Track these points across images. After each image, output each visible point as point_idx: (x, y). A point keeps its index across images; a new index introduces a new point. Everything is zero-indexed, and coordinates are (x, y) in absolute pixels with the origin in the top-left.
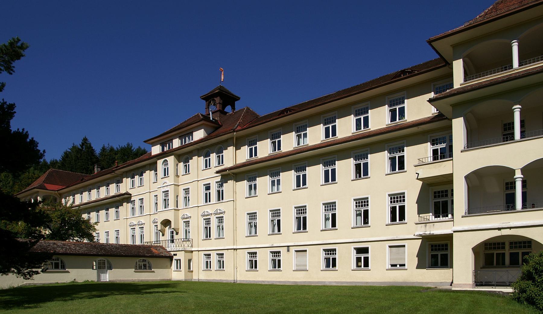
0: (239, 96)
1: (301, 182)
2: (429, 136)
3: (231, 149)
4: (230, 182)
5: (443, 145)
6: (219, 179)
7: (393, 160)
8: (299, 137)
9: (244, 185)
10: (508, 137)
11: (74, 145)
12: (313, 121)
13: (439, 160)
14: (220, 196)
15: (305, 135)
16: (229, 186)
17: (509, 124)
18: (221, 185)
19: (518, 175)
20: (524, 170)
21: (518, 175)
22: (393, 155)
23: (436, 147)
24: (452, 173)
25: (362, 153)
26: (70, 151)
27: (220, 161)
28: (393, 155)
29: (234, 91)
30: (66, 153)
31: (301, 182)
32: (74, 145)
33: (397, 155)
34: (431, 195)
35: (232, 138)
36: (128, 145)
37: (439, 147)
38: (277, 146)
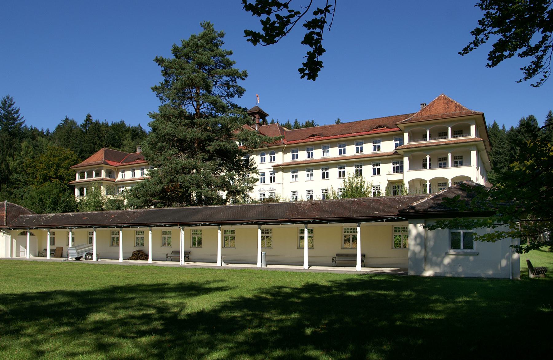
0: (268, 114)
1: (325, 176)
2: (392, 160)
3: (281, 154)
4: (280, 173)
5: (398, 165)
6: (272, 170)
7: (374, 169)
8: (324, 152)
9: (290, 174)
10: (424, 166)
11: (67, 117)
12: (333, 144)
13: (396, 173)
14: (273, 180)
15: (328, 151)
16: (279, 175)
17: (425, 159)
18: (273, 174)
19: (428, 183)
20: (430, 181)
21: (428, 183)
22: (374, 167)
23: (394, 166)
24: (402, 179)
25: (359, 165)
26: (63, 122)
27: (273, 159)
28: (374, 167)
29: (266, 111)
30: (59, 126)
31: (325, 176)
32: (67, 117)
33: (377, 167)
34: (392, 188)
35: (283, 148)
36: (121, 121)
37: (396, 166)
38: (310, 155)
